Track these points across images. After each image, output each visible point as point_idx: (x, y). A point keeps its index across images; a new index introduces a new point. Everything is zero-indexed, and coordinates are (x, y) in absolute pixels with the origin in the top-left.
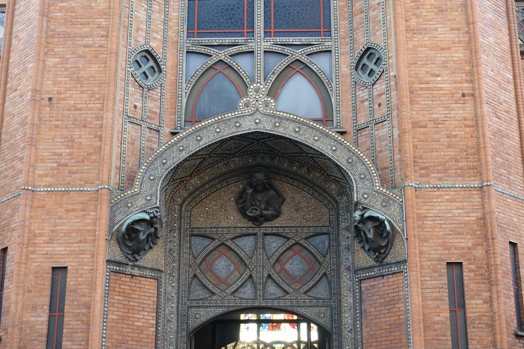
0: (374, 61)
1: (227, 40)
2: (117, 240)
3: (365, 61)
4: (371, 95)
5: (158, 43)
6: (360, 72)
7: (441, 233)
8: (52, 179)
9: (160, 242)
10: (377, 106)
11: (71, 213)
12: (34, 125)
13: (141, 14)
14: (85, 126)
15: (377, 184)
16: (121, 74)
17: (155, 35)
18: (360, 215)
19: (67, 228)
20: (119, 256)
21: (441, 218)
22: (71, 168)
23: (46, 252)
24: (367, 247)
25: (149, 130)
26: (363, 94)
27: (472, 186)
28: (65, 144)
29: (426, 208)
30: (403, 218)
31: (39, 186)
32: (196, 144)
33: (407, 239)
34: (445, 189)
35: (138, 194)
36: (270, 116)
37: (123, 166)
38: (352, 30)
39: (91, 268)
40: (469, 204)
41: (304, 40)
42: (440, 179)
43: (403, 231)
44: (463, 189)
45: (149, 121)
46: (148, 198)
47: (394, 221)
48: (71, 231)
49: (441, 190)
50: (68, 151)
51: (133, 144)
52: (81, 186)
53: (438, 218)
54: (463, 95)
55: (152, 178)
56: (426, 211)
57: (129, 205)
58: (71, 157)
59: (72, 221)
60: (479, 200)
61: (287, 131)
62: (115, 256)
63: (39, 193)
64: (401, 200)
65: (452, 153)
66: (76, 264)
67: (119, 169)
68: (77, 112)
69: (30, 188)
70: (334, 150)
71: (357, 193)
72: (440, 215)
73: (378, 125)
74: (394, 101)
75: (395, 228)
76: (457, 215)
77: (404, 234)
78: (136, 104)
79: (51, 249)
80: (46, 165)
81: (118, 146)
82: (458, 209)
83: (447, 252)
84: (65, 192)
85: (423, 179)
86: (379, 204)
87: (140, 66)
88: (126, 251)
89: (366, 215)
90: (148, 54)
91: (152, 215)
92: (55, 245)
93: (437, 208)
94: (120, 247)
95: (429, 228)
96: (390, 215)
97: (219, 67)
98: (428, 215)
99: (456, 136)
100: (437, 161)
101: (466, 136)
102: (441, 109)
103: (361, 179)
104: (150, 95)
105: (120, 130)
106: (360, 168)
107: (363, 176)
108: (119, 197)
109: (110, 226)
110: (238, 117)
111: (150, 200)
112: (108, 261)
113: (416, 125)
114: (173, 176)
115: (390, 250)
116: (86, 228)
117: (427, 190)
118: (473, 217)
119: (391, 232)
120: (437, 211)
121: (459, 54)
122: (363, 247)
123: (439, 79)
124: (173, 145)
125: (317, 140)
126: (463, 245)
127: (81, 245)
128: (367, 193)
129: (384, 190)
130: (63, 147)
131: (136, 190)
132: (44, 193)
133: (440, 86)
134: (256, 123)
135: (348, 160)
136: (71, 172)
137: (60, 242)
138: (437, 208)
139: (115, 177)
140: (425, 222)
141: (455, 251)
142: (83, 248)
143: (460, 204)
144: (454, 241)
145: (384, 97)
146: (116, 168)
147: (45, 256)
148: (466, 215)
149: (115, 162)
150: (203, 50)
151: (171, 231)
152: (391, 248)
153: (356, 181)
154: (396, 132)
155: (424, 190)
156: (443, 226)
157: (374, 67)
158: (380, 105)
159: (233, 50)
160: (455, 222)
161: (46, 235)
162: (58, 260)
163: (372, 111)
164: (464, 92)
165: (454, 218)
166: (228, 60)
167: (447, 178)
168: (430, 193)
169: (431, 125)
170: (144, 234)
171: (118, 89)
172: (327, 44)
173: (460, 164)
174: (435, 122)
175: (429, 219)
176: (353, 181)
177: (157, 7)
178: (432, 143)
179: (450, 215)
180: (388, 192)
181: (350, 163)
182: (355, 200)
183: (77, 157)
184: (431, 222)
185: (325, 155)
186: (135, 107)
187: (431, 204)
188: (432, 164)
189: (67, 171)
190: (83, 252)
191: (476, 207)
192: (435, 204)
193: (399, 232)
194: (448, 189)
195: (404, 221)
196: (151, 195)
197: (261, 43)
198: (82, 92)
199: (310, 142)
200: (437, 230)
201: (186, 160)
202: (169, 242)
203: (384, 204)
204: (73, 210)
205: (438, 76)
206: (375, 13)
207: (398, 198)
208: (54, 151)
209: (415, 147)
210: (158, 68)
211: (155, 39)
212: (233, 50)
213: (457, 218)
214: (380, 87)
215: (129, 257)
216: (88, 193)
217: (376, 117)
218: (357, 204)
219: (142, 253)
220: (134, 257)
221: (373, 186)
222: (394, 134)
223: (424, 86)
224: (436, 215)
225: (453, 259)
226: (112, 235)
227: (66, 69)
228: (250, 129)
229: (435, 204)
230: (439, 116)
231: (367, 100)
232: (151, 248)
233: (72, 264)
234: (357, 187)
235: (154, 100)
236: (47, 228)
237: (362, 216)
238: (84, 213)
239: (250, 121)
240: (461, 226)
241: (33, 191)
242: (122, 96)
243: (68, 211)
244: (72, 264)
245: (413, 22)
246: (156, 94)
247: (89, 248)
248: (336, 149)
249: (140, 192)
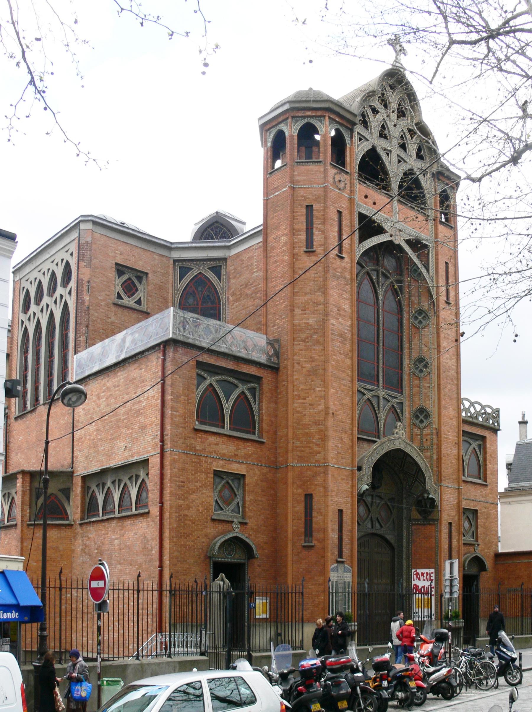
1: (371, 387)
26: (417, 431)
42: (448, 483)
145: (429, 436)
150: (363, 390)
154: (435, 457)
158: (427, 440)
197: (383, 393)
205: (449, 432)
206: (426, 391)
214: (426, 431)
237: (428, 497)
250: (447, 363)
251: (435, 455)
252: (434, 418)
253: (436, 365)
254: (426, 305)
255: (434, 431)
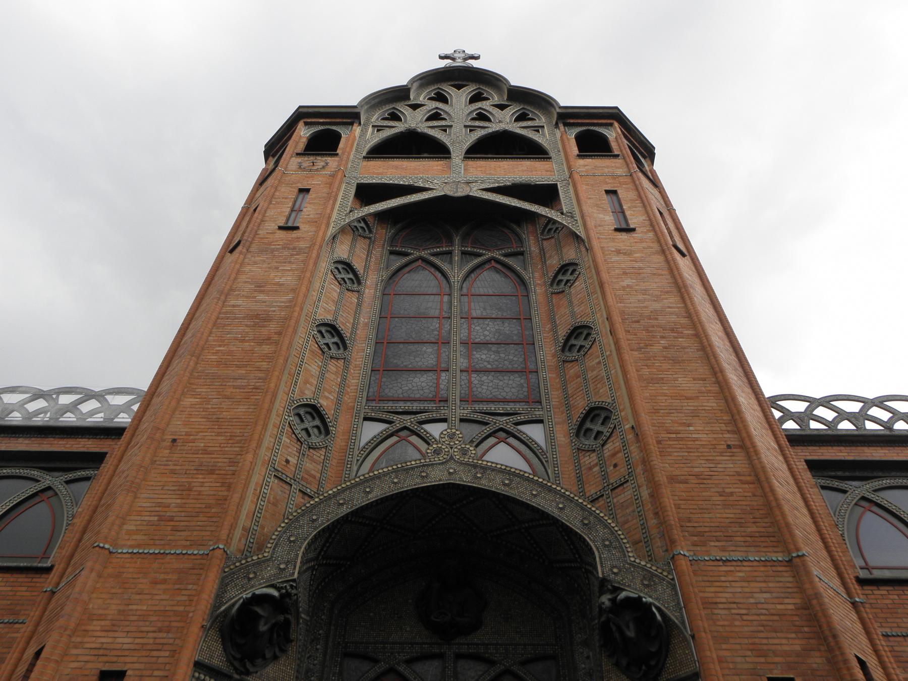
0: (600, 421)
2: (221, 631)
3: (588, 425)
4: (600, 458)
5: (330, 404)
6: (583, 439)
7: (746, 629)
8: (144, 537)
9: (293, 650)
10: (612, 468)
11: (159, 586)
12: (141, 467)
13: (314, 369)
14: (211, 472)
15: (631, 554)
16: (274, 419)
17: (326, 394)
18: (609, 600)
19: (145, 608)
20: (218, 659)
21: (740, 606)
22: (178, 524)
23: (98, 646)
24: (624, 662)
25: (301, 495)
26: (589, 459)
27: (774, 559)
28: (179, 492)
29: (712, 589)
30: (679, 603)
31: (123, 546)
32: (363, 498)
33: (693, 637)
34: (734, 563)
35: (268, 560)
36: (469, 465)
37: (255, 528)
38: (567, 398)
39: (166, 674)
40: (778, 585)
41: (509, 407)
42: (723, 549)
43: (683, 623)
44: (762, 563)
45: (302, 483)
46: (282, 566)
47: (667, 608)
48: (151, 613)
49: (729, 564)
50: (179, 501)
51: (274, 504)
52: (185, 547)
53: (734, 606)
54: (729, 447)
55: (292, 539)
56: (713, 595)
57: (251, 576)
58: (181, 509)
59: (157, 597)
60: (791, 579)
61: (494, 484)
62: (211, 657)
63: (119, 556)
64: (671, 577)
65: (732, 516)
66: (142, 666)
67: (246, 530)
68: (206, 456)
69: (107, 546)
70: (561, 508)
71: (602, 566)
72: (736, 601)
73: (616, 491)
74: (636, 454)
75: (670, 619)
76: (763, 601)
77: (685, 628)
78: (289, 458)
79: (110, 640)
80: (143, 518)
81: (252, 501)
82: (762, 592)
83: (762, 660)
84: (159, 556)
85: (698, 548)
86: (638, 581)
87: (302, 421)
88: (233, 653)
89: (623, 595)
90: (314, 410)
91: (284, 591)
92: (116, 635)
93: (730, 590)
94: (223, 644)
95: (724, 620)
96: (656, 599)
97: (404, 433)
98: (718, 600)
99: (732, 494)
100: (712, 525)
101: (746, 494)
102: (703, 462)
103: (606, 546)
104: (310, 454)
105: (261, 482)
106: (602, 532)
107: (607, 543)
108: (238, 564)
109: (215, 606)
110: (424, 465)
111: (284, 569)
112: (198, 665)
113: (672, 479)
114: (324, 546)
115: (665, 660)
116: (175, 608)
117: (707, 563)
118: (790, 604)
119: (663, 625)
120: (731, 595)
121: (711, 403)
122: (617, 664)
123: (691, 428)
124: (330, 498)
125: (535, 496)
126: (786, 648)
127: (161, 635)
128: (616, 563)
129: (643, 563)
130: (174, 496)
131: (266, 555)
132: (127, 556)
133: (694, 436)
134: (450, 473)
135: (582, 521)
136: (175, 529)
137: (127, 629)
138: (730, 590)
139: (240, 540)
140: (716, 611)
141: (777, 659)
142: (162, 641)
143: (764, 585)
144: (771, 641)
145: (620, 455)
146: (244, 529)
147: (96, 652)
148: (776, 601)
149: (243, 520)
150: (384, 416)
151: (313, 641)
152: (666, 656)
153: (597, 549)
154: (645, 493)
155: (702, 563)
156: (745, 617)
157: (601, 429)
158: (615, 466)
159: (423, 417)
160: (764, 611)
161: (109, 617)
162: (115, 659)
163: (605, 476)
164: (729, 443)
165: (760, 606)
166: (416, 428)
167: (734, 548)
168: (714, 568)
169: (693, 480)
170: (265, 625)
171: (268, 433)
172: (538, 413)
173: (749, 530)
174: (696, 476)
175: (721, 606)
176: (594, 549)
177: (335, 369)
178: (700, 503)
179: (752, 601)
180: (649, 565)
181: (586, 524)
182: (600, 575)
183: (189, 510)
184: (726, 612)
185: (548, 515)
186: (287, 461)
187: (718, 584)
188: (707, 529)
189: (169, 528)
190: (160, 647)
191: (790, 590)
192: (724, 584)
193: (677, 626)
194: (739, 564)
195: (681, 609)
196: (287, 563)
198: (218, 434)
199: (525, 497)
200: (737, 623)
201: (345, 519)
202: (308, 658)
203: (646, 582)
204: (164, 581)
207: (665, 574)
208: (160, 501)
209: (678, 507)
210: (325, 429)
211: (327, 398)
212: (423, 417)
213: (765, 606)
215: (236, 664)
216: (193, 557)
217: (611, 481)
218: (604, 581)
219: (259, 661)
220: (244, 666)
221: (625, 556)
222: (642, 494)
223: (674, 436)
224: (730, 600)
225: (775, 671)
226: (215, 621)
227: (205, 410)
228: (440, 480)
229: (724, 584)
230: (702, 470)
231: (596, 465)
232: (275, 658)
233: (137, 666)
234: (600, 558)
235: (313, 460)
236: (113, 607)
237: (613, 601)
238: (177, 586)
239: (440, 470)
240: (776, 618)
241: (110, 553)
242: (272, 444)
243: (155, 582)
244: (137, 666)
245: (646, 371)
246: (319, 455)
247: (171, 641)
248: (565, 506)
249: (272, 557)
250: (646, 307)
251: (645, 488)
252: (623, 410)
253: (605, 316)
254: (570, 254)
255: (631, 436)
